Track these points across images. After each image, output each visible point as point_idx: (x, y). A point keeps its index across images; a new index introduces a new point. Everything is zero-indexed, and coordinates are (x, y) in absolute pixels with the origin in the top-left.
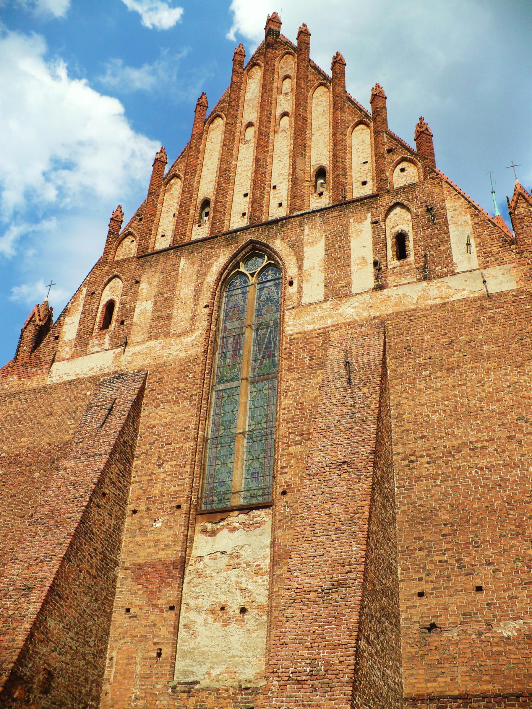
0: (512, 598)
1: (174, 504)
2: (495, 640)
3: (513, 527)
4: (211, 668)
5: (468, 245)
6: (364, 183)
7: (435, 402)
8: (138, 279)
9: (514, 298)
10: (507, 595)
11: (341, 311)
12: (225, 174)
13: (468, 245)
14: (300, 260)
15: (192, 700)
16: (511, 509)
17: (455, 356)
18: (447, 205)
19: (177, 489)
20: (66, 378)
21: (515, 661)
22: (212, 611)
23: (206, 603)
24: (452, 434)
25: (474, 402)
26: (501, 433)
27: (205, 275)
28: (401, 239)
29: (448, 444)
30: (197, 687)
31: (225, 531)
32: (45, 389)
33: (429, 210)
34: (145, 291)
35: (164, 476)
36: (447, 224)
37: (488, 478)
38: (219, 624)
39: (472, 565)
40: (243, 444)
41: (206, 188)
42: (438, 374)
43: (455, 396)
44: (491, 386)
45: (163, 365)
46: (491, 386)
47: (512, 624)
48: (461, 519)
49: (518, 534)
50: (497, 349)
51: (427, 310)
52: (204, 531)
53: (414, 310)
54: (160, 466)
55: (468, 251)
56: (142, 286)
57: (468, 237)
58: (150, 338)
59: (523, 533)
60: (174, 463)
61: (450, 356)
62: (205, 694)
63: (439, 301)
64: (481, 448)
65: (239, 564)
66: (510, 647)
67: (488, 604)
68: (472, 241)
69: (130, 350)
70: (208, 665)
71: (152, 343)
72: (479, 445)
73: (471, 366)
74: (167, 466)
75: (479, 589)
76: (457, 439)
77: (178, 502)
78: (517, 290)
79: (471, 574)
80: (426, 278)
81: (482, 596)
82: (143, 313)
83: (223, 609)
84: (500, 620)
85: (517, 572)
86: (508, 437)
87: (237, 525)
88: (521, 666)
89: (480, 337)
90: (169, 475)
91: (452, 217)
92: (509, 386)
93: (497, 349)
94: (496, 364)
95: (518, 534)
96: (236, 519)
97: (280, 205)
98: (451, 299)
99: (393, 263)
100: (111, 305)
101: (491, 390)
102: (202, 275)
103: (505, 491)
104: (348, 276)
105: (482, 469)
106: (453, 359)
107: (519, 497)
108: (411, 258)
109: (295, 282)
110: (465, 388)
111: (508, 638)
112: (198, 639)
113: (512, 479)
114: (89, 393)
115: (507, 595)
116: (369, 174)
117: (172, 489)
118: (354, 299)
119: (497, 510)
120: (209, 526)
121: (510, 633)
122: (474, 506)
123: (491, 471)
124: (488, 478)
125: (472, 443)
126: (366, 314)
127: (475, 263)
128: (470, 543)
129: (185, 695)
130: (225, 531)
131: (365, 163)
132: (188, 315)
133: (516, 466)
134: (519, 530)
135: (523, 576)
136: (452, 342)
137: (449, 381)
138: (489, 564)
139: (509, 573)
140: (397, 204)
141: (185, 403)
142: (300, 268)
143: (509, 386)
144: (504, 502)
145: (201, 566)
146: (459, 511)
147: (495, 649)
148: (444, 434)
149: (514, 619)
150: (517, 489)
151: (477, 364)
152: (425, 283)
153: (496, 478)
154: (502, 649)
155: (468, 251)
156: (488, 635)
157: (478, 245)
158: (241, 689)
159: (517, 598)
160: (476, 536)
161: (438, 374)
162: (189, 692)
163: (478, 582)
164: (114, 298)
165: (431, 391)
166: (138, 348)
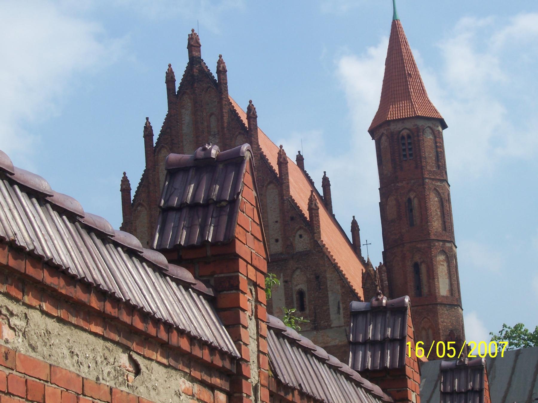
5: (339, 308)
6: (277, 241)
13: (339, 308)
18: (327, 276)
28: (301, 294)
33: (317, 277)
36: (327, 291)
55: (339, 312)
57: (339, 303)
68: (341, 305)
91: (330, 286)
98: (330, 345)
108: (307, 311)
116: (280, 233)
127: (342, 321)
131: (277, 222)
140: (297, 268)
155: (339, 312)
157: (344, 309)
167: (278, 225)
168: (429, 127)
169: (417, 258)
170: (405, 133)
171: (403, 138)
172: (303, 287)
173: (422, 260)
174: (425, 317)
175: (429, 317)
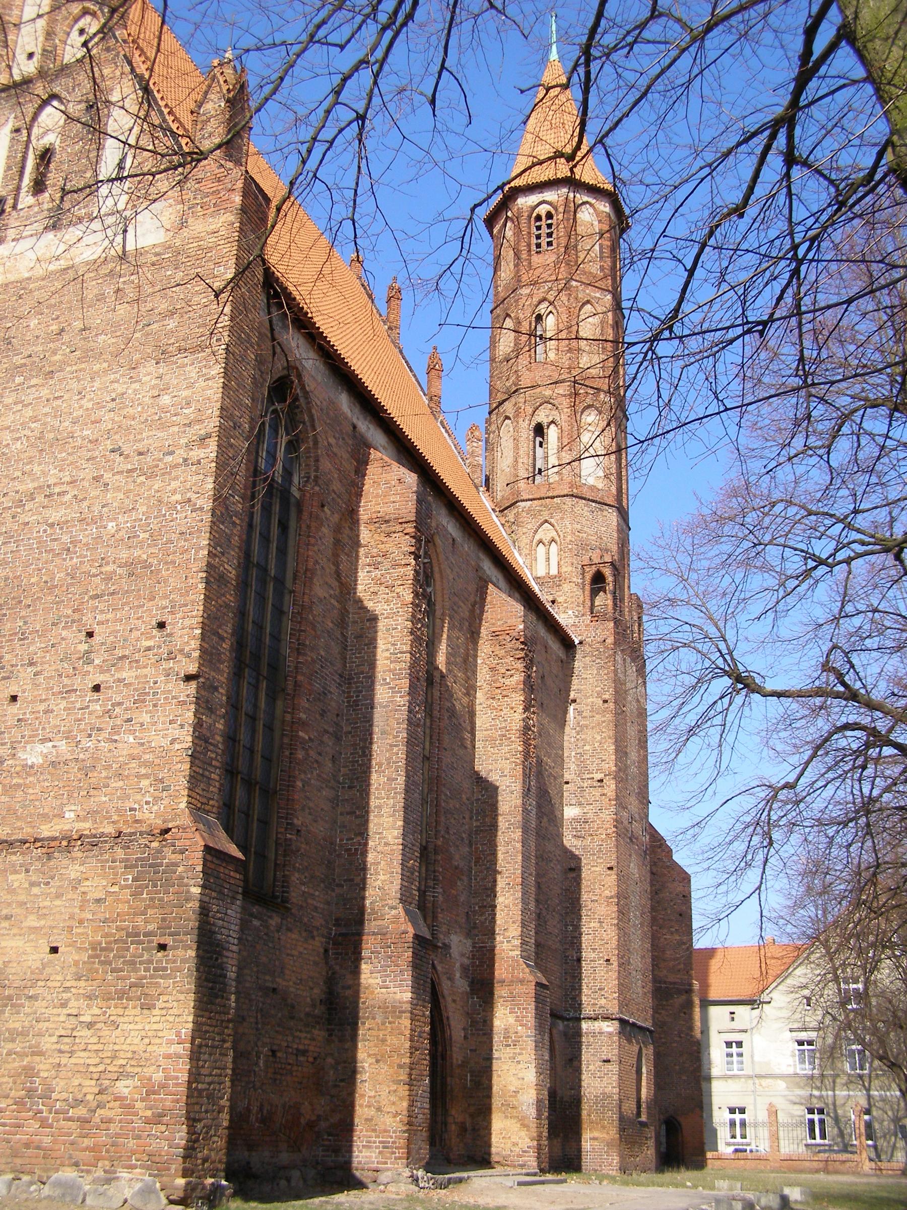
0: (47, 711)
2: (18, 769)
3: (70, 612)
7: (21, 424)
9: (155, 259)
10: (42, 707)
16: (72, 584)
17: (61, 352)
21: (32, 797)
24: (31, 473)
25: (67, 424)
26: (87, 472)
29: (22, 488)
37: (55, 540)
39: (12, 666)
42: (34, 381)
43: (46, 414)
44: (92, 399)
46: (92, 399)
47: (40, 748)
48: (14, 598)
49: (73, 621)
50: (114, 340)
51: (43, 279)
53: (29, 279)
59: (80, 620)
61: (54, 353)
64: (59, 494)
66: (31, 779)
67: (19, 720)
72: (57, 490)
73: (75, 368)
75: (14, 698)
76: (33, 481)
78: (162, 245)
79: (9, 678)
81: (14, 709)
84: (27, 742)
85: (60, 676)
86: (94, 478)
88: (37, 803)
89: (99, 321)
92: (113, 400)
93: (114, 340)
94: (105, 365)
95: (73, 621)
101: (90, 405)
103: (72, 558)
105: (52, 525)
106: (58, 357)
107: (86, 567)
110: (59, 402)
111: (32, 767)
113: (84, 541)
115: (42, 707)
119: (56, 586)
121: (34, 760)
122: (33, 580)
123: (61, 528)
124: (55, 540)
125: (49, 486)
128: (15, 634)
134: (76, 616)
135: (66, 681)
136: (63, 330)
137: (45, 392)
138: (31, 664)
139: (51, 677)
143: (113, 400)
144: (68, 574)
146: (13, 588)
147: (14, 781)
148: (19, 474)
149: (43, 741)
150: (86, 556)
151: (83, 366)
152: (50, 235)
153: (66, 538)
154: (21, 781)
156: (10, 762)
159: (52, 711)
160: (25, 623)
161: (34, 381)
163: (14, 690)
165: (19, 407)
168: (587, 202)
169: (542, 417)
170: (543, 210)
171: (539, 218)
172: (51, 139)
173: (551, 419)
174: (546, 521)
175: (552, 521)
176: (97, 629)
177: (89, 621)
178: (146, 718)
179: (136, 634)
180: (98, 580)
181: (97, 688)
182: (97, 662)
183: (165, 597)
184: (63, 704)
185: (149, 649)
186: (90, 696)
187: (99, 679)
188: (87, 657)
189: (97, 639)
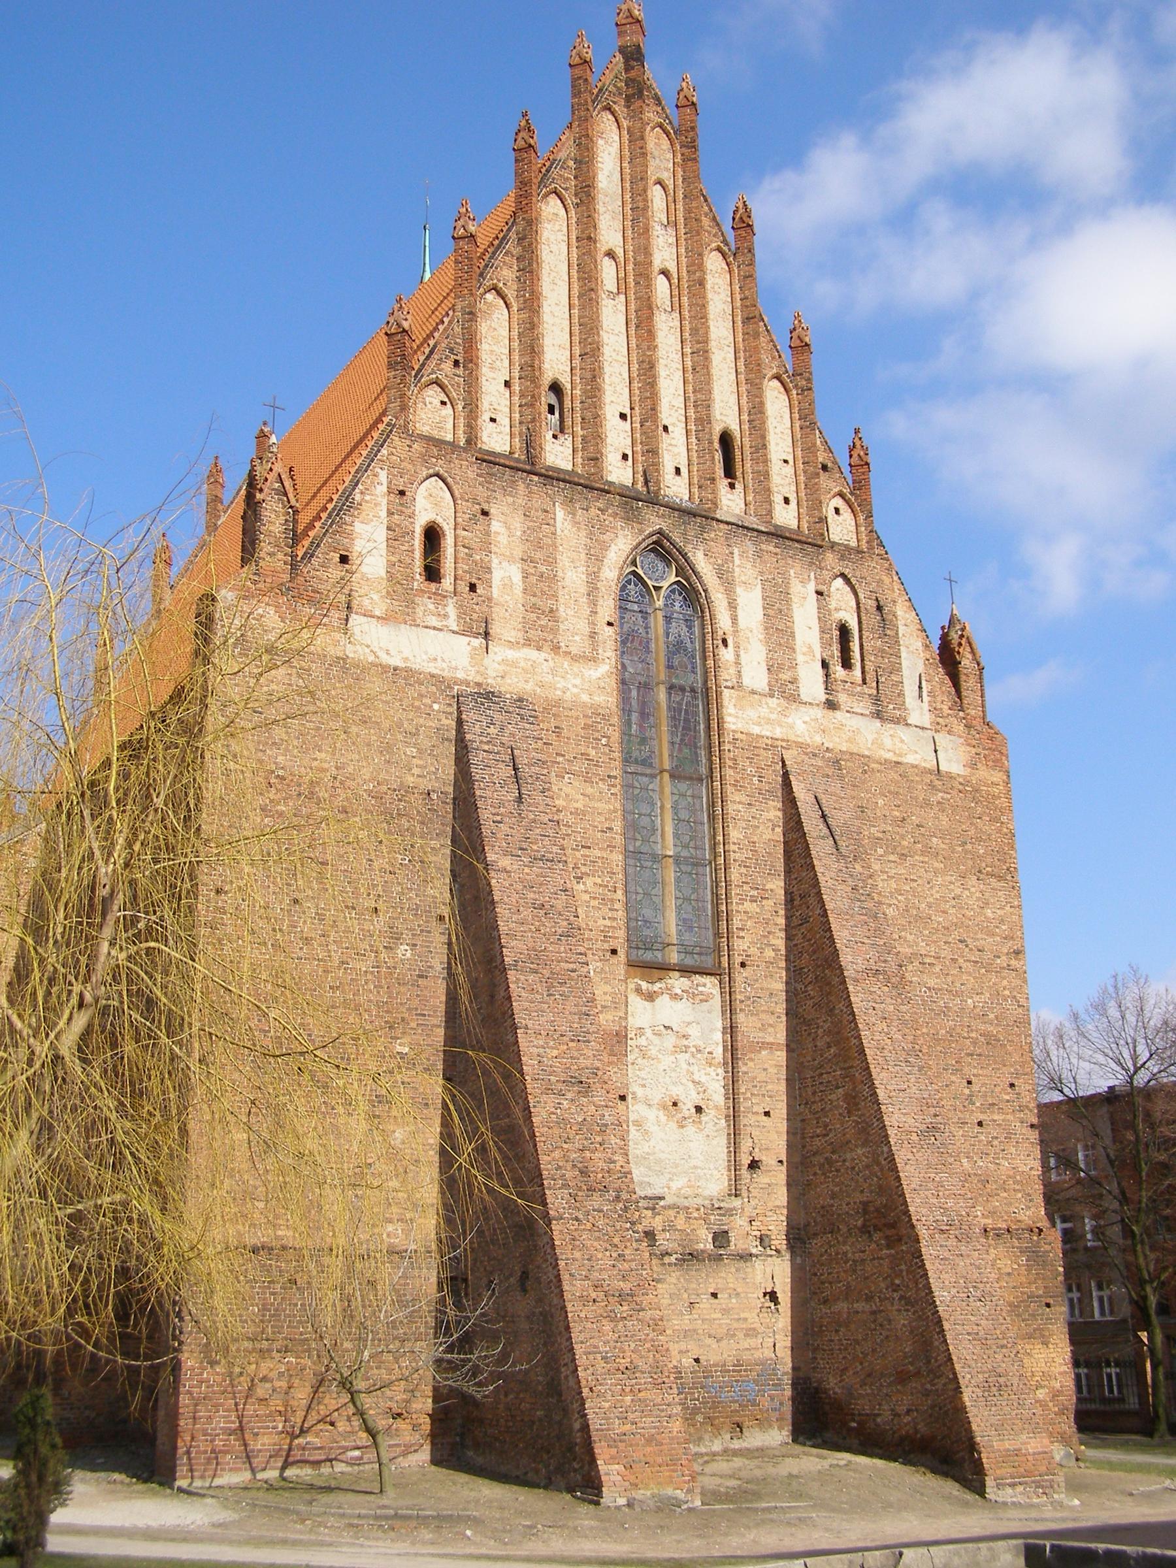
1: (606, 946)
4: (671, 1179)
5: (920, 687)
8: (486, 507)
11: (790, 720)
12: (588, 350)
14: (732, 606)
15: (658, 1218)
19: (608, 923)
20: (385, 659)
22: (665, 1108)
23: (656, 1096)
27: (600, 560)
30: (662, 1203)
31: (666, 997)
32: (342, 661)
34: (503, 539)
35: (586, 897)
38: (673, 1125)
40: (671, 874)
41: (556, 361)
42: (892, 858)
45: (558, 703)
52: (638, 990)
54: (579, 878)
56: (496, 526)
58: (528, 643)
60: (599, 881)
61: (903, 837)
62: (672, 1213)
63: (889, 756)
65: (687, 1047)
69: (499, 652)
70: (668, 1176)
71: (533, 654)
74: (589, 881)
77: (613, 944)
80: (878, 715)
82: (507, 585)
83: (675, 1104)
87: (679, 991)
90: (595, 898)
96: (678, 983)
97: (678, 471)
99: (839, 671)
100: (432, 535)
102: (595, 557)
104: (794, 667)
105: (929, 989)
107: (958, 1030)
109: (730, 642)
110: (915, 884)
112: (652, 1143)
114: (436, 707)
117: (601, 922)
118: (803, 708)
120: (644, 985)
126: (818, 739)
129: (649, 1213)
130: (666, 997)
132: (583, 627)
133: (957, 994)
141: (601, 784)
142: (734, 620)
145: (642, 1041)
158: (713, 1208)
161: (892, 858)
162: (654, 1209)
164: (439, 520)
166: (511, 654)
167: (789, 470)
176: (973, 1079)
177: (969, 1072)
178: (1013, 1150)
179: (998, 1089)
180: (968, 1042)
181: (980, 1124)
182: (978, 1104)
183: (1012, 1066)
184: (961, 1133)
185: (1008, 1101)
186: (977, 1129)
187: (982, 1117)
188: (970, 1099)
189: (975, 1088)
